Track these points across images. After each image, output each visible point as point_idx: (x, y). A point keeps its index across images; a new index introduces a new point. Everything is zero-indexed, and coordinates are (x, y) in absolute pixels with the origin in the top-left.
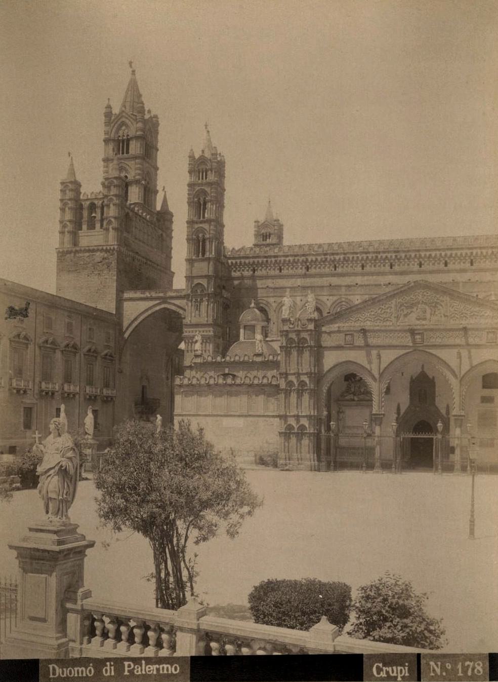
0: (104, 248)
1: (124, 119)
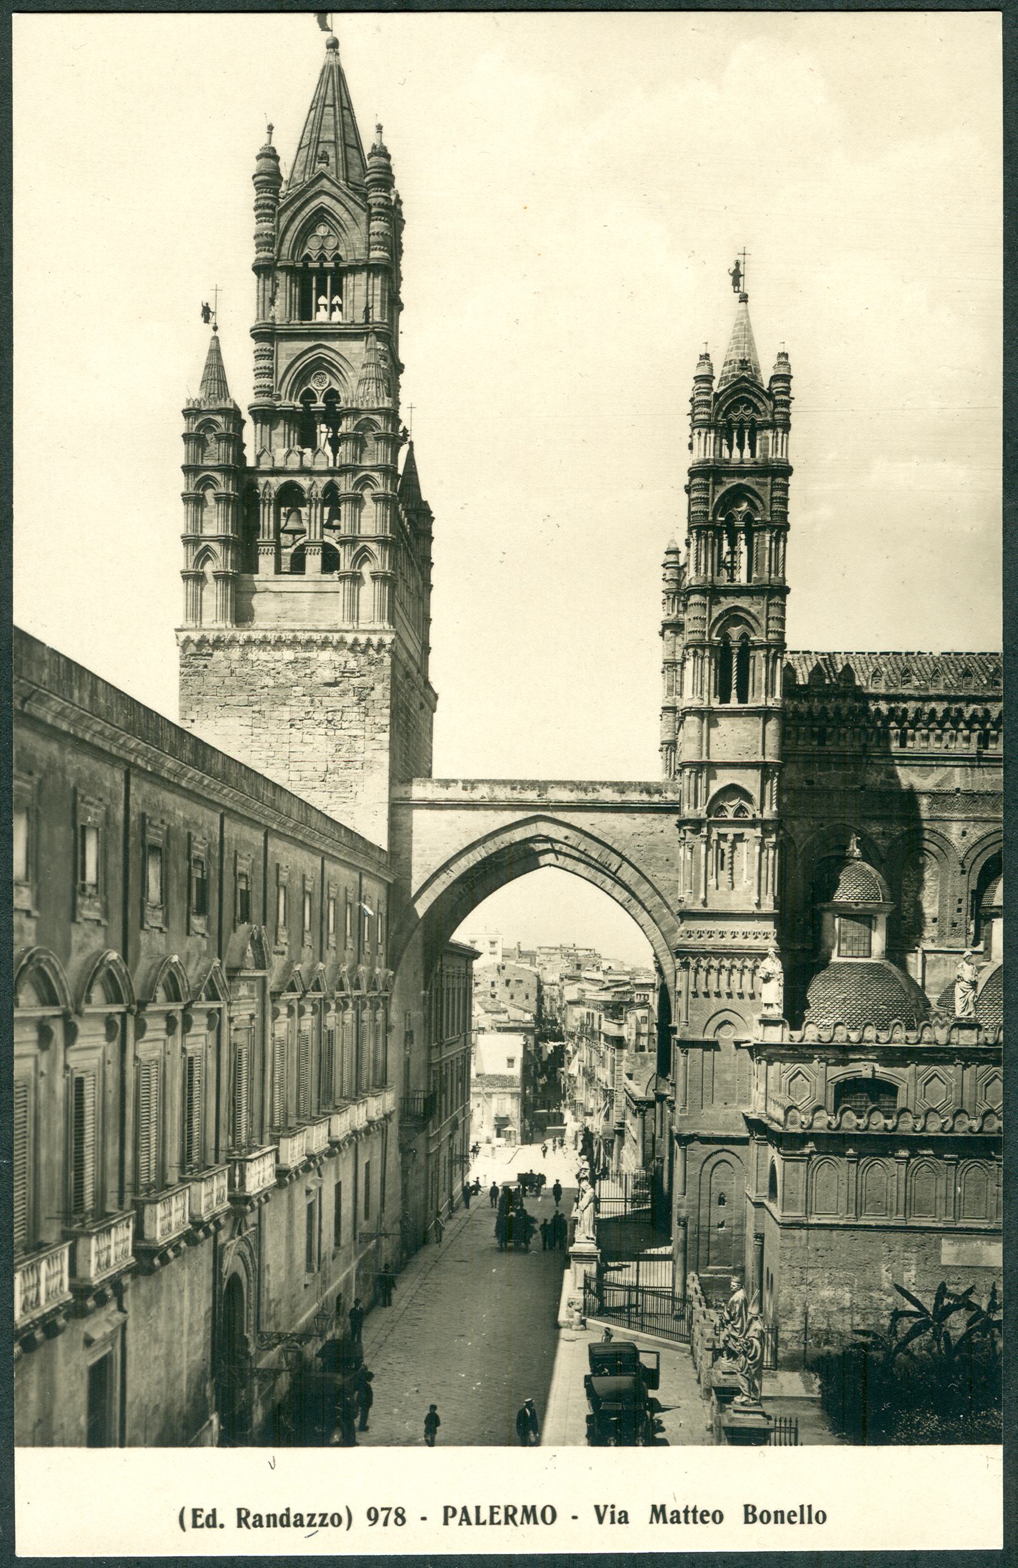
0: (349, 638)
1: (325, 200)
